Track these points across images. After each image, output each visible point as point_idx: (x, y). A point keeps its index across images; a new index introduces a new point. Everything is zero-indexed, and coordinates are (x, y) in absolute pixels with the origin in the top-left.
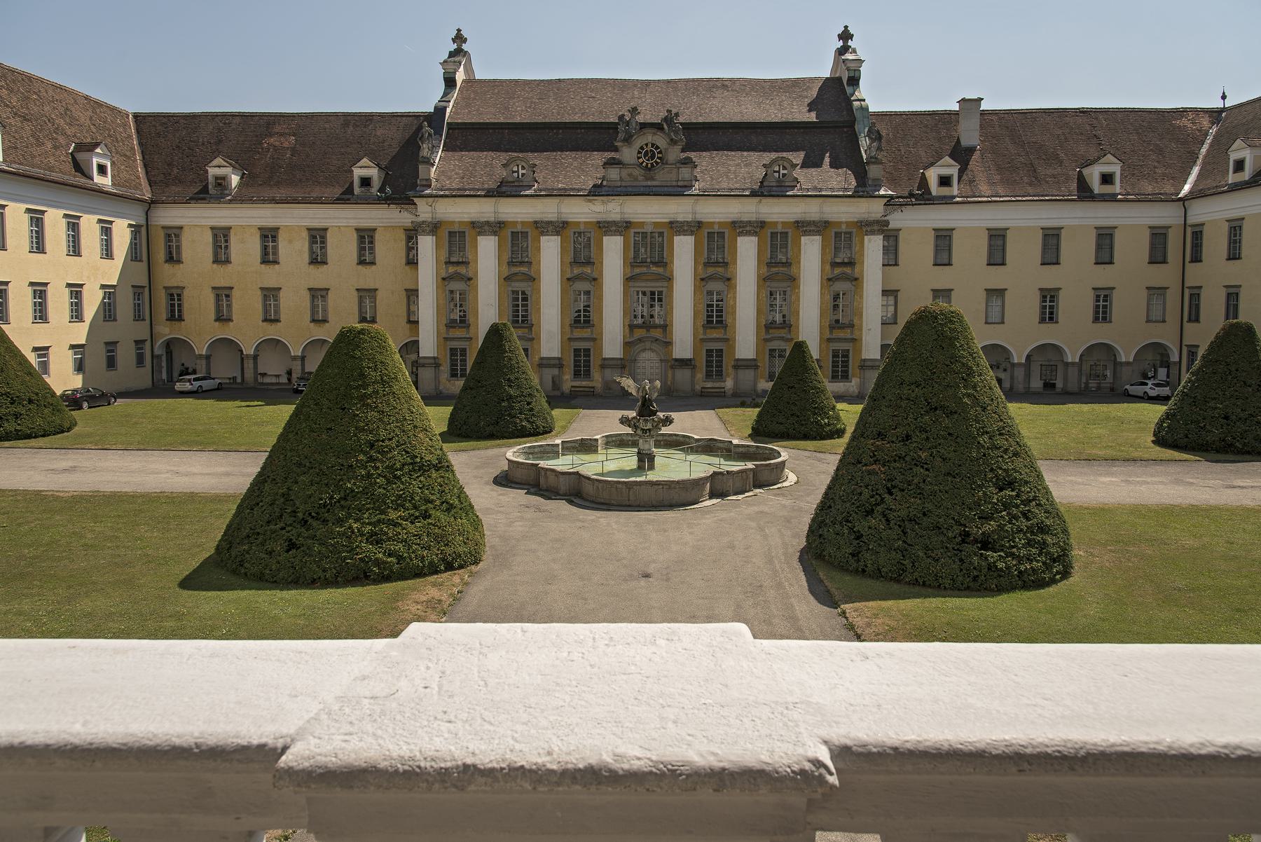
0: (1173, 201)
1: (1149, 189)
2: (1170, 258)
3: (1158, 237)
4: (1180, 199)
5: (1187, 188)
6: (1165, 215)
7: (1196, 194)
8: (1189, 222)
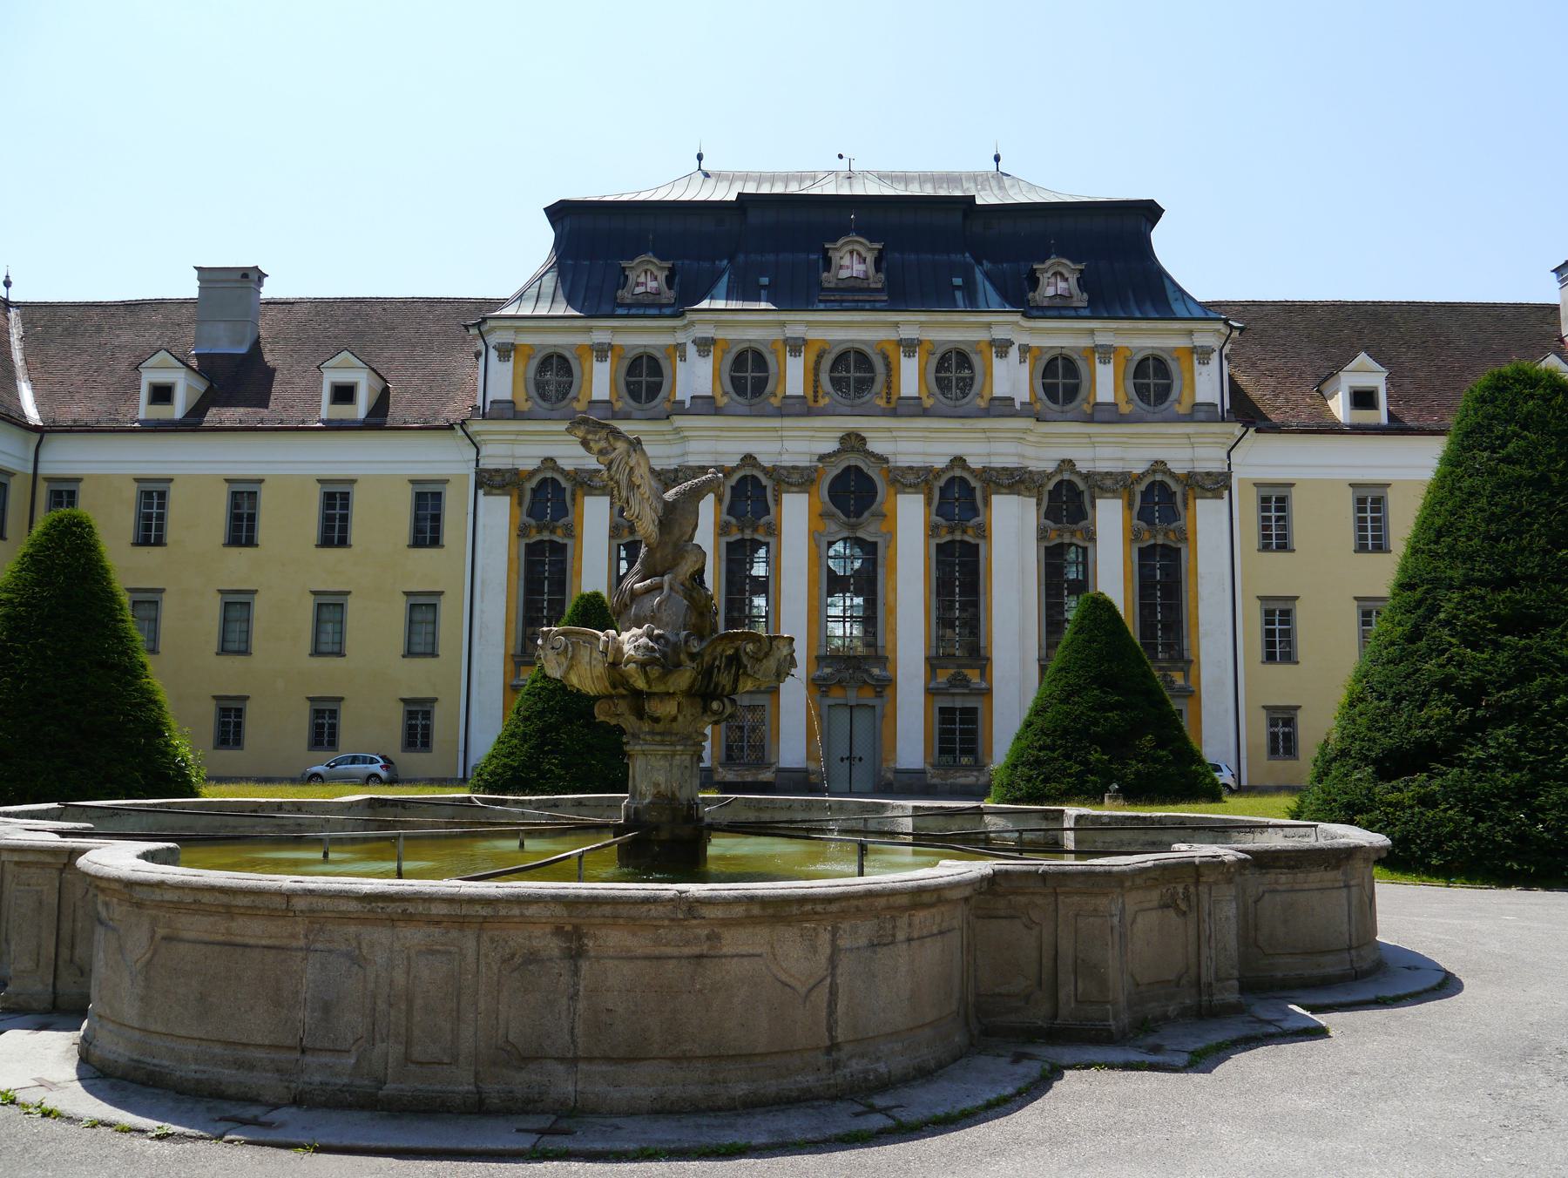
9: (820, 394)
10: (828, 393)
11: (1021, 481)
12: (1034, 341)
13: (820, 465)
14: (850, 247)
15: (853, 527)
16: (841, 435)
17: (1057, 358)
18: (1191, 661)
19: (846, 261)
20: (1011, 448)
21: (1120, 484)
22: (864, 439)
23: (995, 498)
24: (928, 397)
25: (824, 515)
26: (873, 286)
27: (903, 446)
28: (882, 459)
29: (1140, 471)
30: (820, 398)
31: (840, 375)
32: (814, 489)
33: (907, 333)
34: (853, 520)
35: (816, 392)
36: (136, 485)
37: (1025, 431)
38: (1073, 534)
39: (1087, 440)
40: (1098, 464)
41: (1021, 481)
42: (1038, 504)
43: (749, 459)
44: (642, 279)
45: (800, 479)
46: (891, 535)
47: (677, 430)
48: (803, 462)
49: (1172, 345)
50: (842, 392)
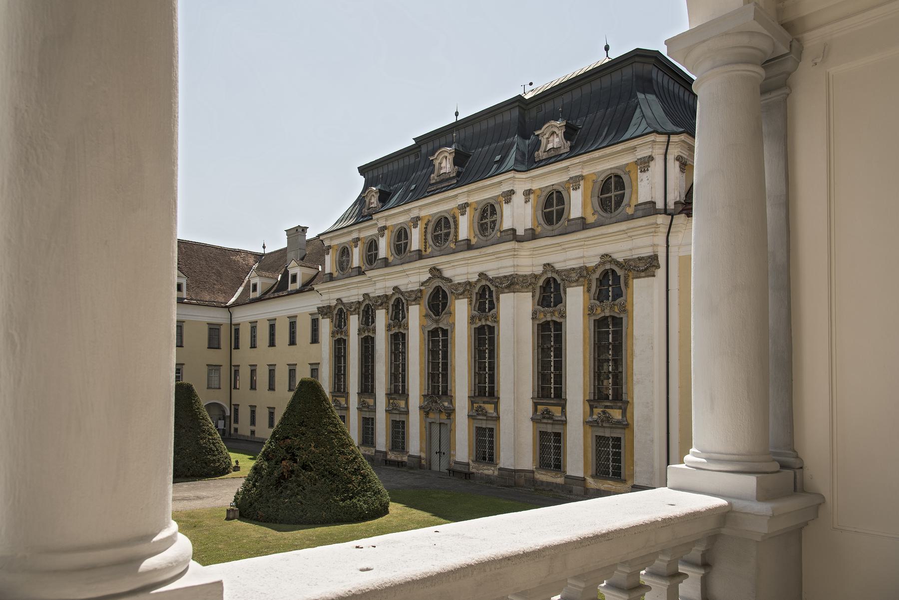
0: (222, 307)
1: (207, 298)
2: (222, 346)
3: (214, 330)
4: (226, 307)
5: (233, 300)
6: (218, 316)
7: (236, 304)
8: (233, 322)
9: (428, 246)
10: (430, 245)
11: (512, 284)
12: (535, 186)
13: (423, 288)
14: (443, 155)
15: (437, 321)
16: (428, 270)
17: (553, 193)
18: (628, 402)
19: (443, 165)
20: (509, 262)
21: (582, 274)
22: (438, 270)
23: (501, 296)
24: (474, 237)
25: (426, 316)
26: (451, 176)
27: (459, 270)
28: (449, 280)
29: (594, 264)
30: (427, 249)
31: (438, 233)
32: (421, 302)
33: (461, 201)
34: (437, 317)
35: (426, 246)
36: (250, 324)
37: (514, 250)
38: (553, 313)
39: (625, 236)
40: (634, 252)
41: (512, 284)
42: (533, 296)
43: (396, 289)
44: (372, 201)
45: (416, 297)
46: (454, 324)
47: (370, 278)
48: (416, 287)
49: (624, 163)
50: (438, 242)
